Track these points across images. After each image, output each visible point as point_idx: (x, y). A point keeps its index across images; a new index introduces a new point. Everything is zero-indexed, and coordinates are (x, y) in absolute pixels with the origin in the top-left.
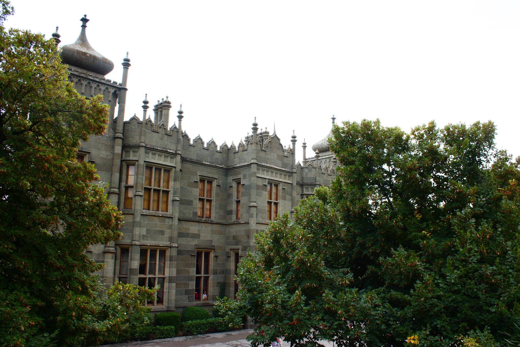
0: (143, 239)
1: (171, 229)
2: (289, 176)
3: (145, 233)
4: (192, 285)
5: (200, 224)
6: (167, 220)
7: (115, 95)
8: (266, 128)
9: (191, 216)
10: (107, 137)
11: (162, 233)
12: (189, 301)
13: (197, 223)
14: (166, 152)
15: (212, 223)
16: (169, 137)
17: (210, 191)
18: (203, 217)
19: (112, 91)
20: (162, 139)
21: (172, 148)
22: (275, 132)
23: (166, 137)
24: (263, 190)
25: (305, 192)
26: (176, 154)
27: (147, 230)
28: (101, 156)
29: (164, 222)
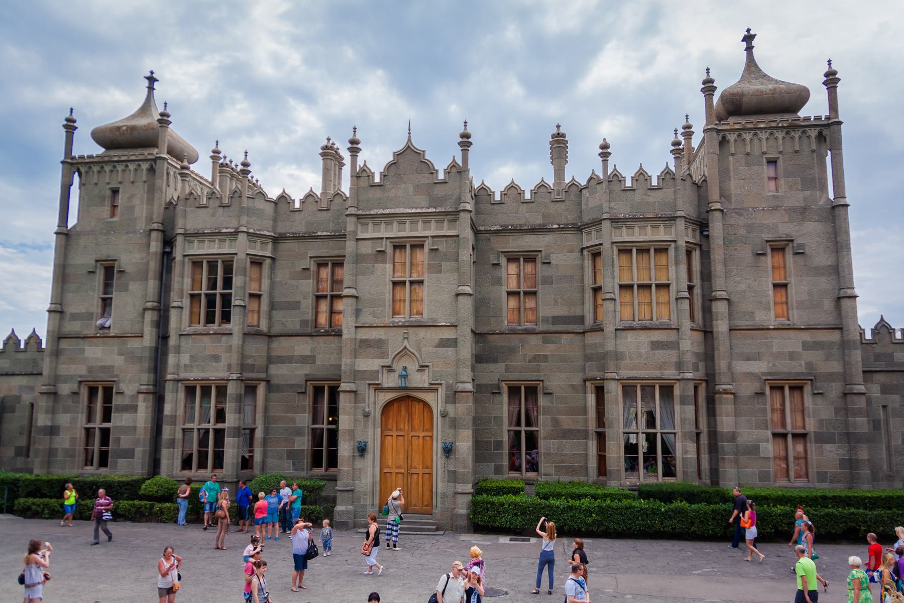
0: (186, 371)
1: (230, 352)
2: (450, 221)
3: (188, 362)
4: (304, 443)
5: (315, 339)
6: (225, 338)
7: (152, 170)
8: (558, 127)
9: (298, 326)
10: (141, 233)
11: (216, 358)
12: (296, 470)
13: (308, 338)
14: (220, 233)
16: (226, 209)
19: (145, 166)
20: (213, 215)
22: (409, 140)
23: (221, 209)
24: (376, 261)
25: (586, 244)
26: (237, 233)
27: (191, 356)
28: (134, 261)
29: (220, 341)
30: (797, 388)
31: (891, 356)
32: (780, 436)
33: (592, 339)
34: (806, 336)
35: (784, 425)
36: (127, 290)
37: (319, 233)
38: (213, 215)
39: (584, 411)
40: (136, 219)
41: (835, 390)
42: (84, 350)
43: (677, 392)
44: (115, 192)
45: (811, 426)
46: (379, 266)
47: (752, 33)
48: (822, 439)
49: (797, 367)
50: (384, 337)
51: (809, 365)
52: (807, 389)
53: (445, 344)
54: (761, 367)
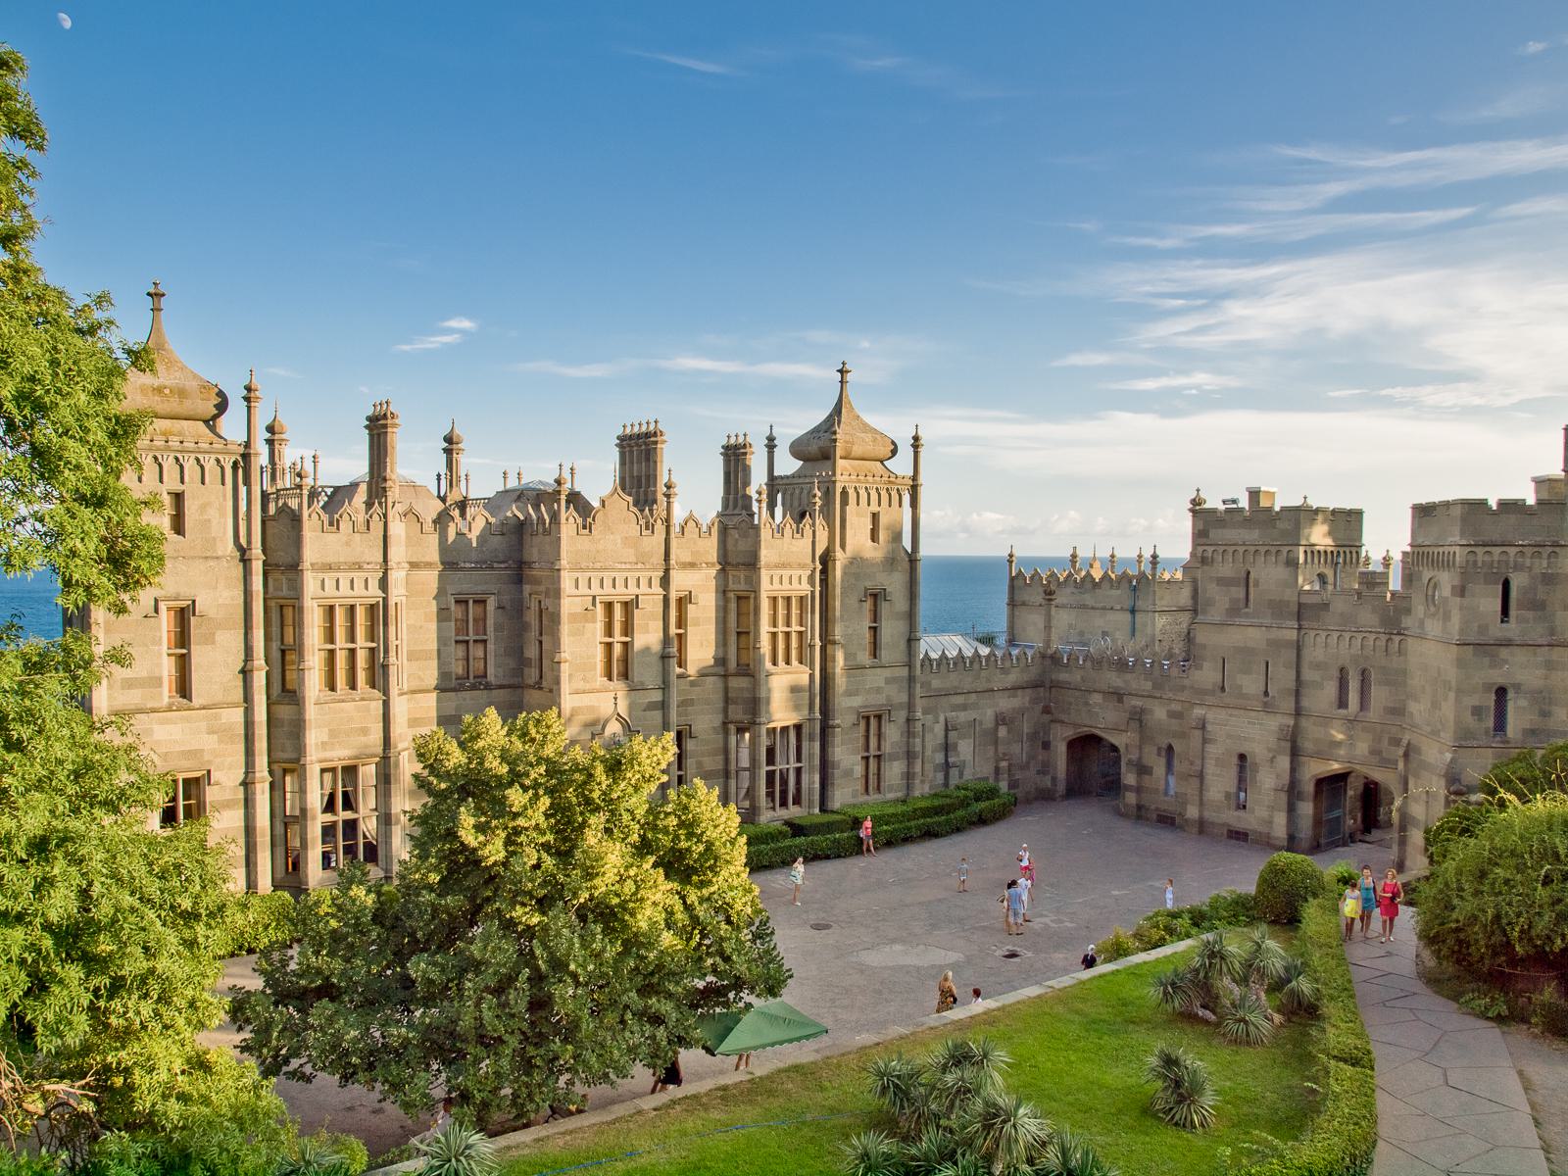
3: (326, 739)
15: (488, 687)
17: (482, 620)
18: (468, 678)
21: (372, 559)
24: (587, 621)
28: (221, 601)
30: (879, 717)
31: (929, 683)
32: (867, 758)
33: (737, 683)
34: (887, 673)
35: (867, 748)
36: (213, 643)
37: (462, 565)
38: (347, 544)
39: (726, 751)
40: (214, 539)
41: (901, 716)
42: (152, 730)
43: (805, 731)
44: (178, 498)
45: (887, 748)
46: (589, 626)
47: (847, 367)
48: (893, 757)
49: (881, 700)
50: (596, 704)
51: (888, 698)
52: (885, 718)
53: (651, 706)
54: (857, 702)
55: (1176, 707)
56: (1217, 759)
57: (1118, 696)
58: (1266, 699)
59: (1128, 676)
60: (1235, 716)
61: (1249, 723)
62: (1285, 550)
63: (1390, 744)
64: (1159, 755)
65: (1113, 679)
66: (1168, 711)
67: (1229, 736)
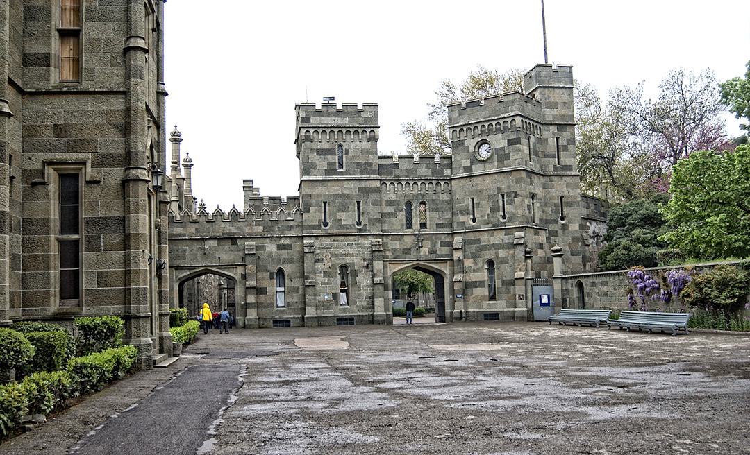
55: (282, 241)
56: (324, 272)
57: (234, 240)
58: (359, 227)
59: (241, 224)
60: (337, 241)
61: (348, 244)
62: (368, 131)
63: (441, 246)
64: (271, 278)
65: (231, 229)
66: (278, 245)
67: (333, 255)
